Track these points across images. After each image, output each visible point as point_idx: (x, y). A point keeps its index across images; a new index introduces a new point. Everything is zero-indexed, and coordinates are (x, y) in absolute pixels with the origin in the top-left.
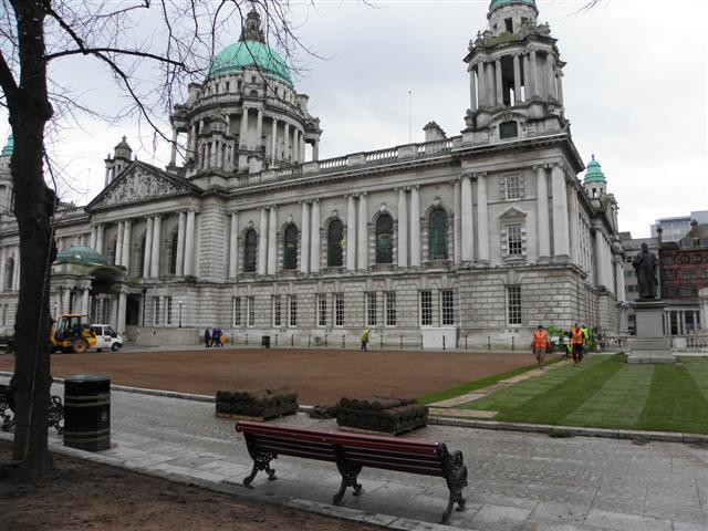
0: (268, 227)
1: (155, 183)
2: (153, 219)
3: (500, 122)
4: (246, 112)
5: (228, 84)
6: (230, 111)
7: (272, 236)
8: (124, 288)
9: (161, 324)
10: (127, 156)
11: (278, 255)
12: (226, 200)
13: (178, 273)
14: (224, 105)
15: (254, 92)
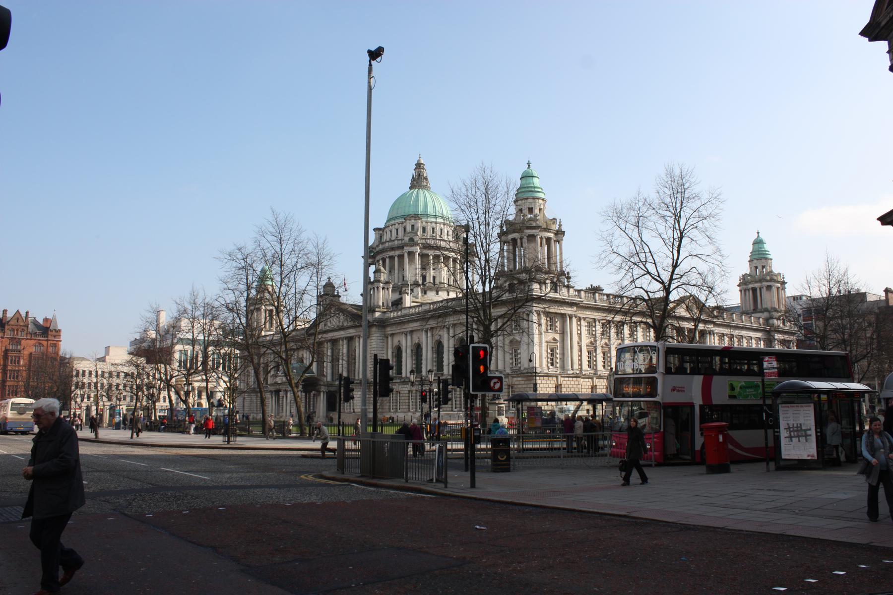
0: (406, 344)
1: (342, 317)
2: (343, 340)
3: (508, 283)
4: (406, 255)
5: (397, 230)
6: (397, 253)
7: (409, 351)
8: (323, 388)
9: (348, 410)
10: (331, 293)
11: (412, 364)
12: (384, 327)
13: (357, 378)
14: (393, 249)
15: (411, 240)
